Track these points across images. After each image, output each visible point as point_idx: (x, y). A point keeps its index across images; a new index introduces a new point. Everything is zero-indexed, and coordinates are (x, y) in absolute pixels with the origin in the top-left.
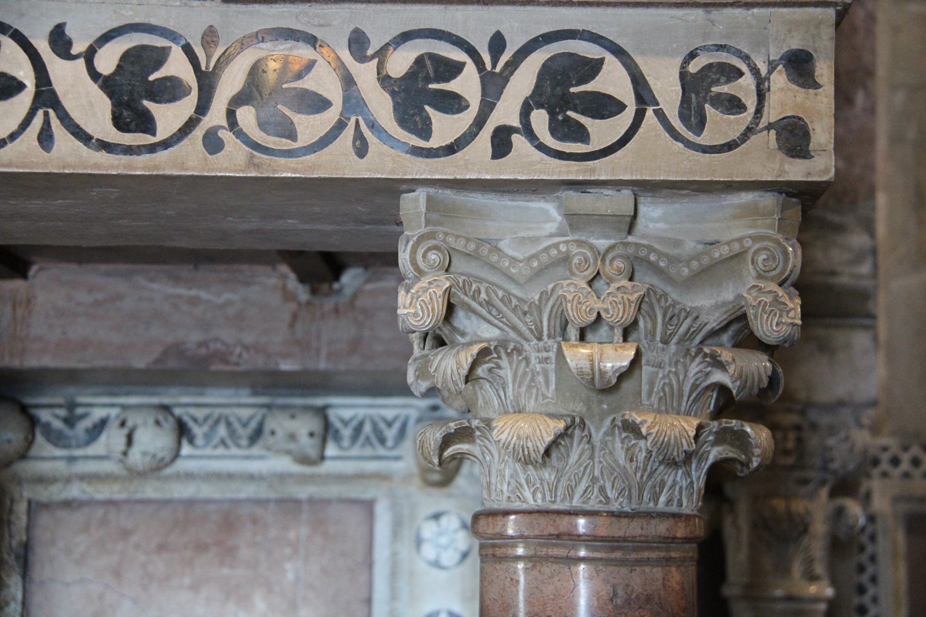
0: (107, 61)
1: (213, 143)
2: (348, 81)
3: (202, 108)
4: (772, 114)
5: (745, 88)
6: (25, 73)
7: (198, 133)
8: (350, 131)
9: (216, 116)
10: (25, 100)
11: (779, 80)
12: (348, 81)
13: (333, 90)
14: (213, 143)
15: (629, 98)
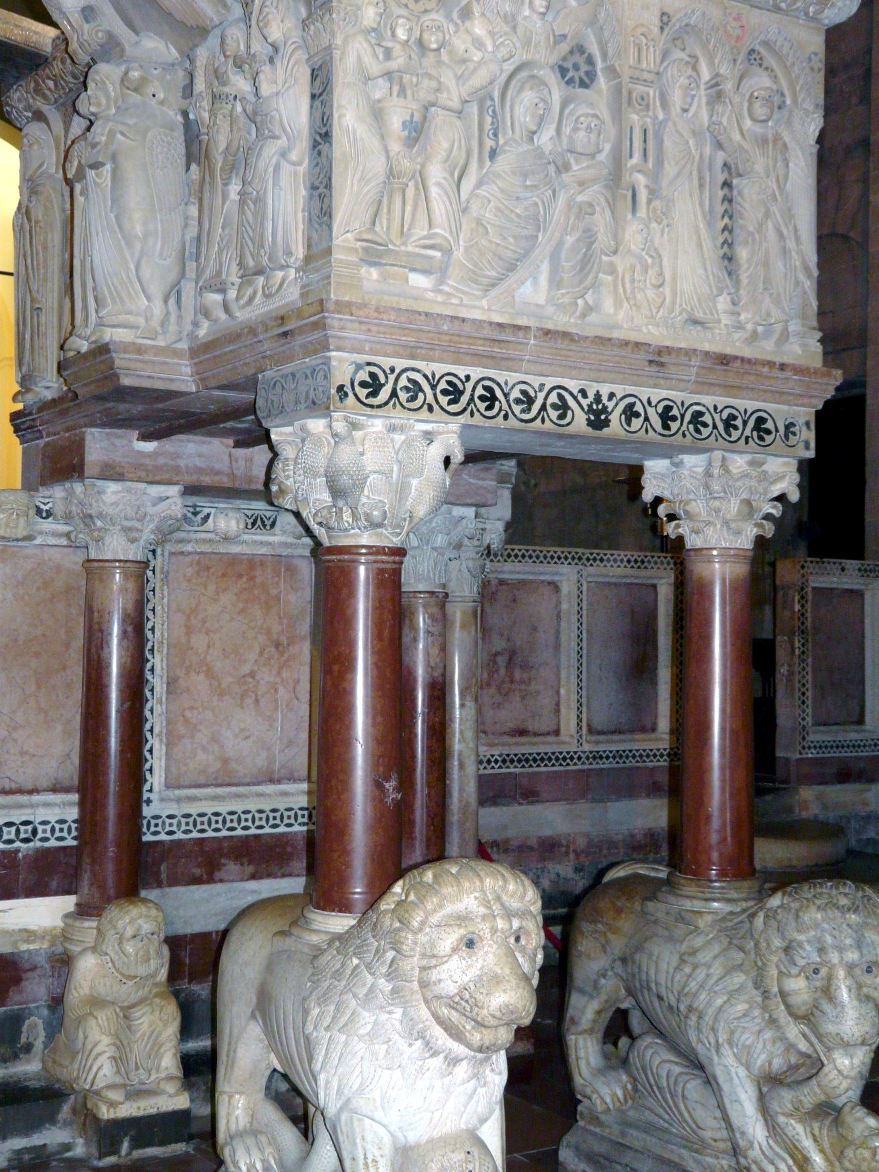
0: (660, 409)
1: (684, 435)
2: (713, 419)
3: (682, 424)
4: (803, 438)
5: (796, 429)
6: (642, 411)
7: (681, 432)
8: (713, 436)
9: (684, 428)
10: (642, 419)
11: (804, 428)
12: (713, 419)
13: (710, 422)
14: (684, 435)
15: (773, 429)
